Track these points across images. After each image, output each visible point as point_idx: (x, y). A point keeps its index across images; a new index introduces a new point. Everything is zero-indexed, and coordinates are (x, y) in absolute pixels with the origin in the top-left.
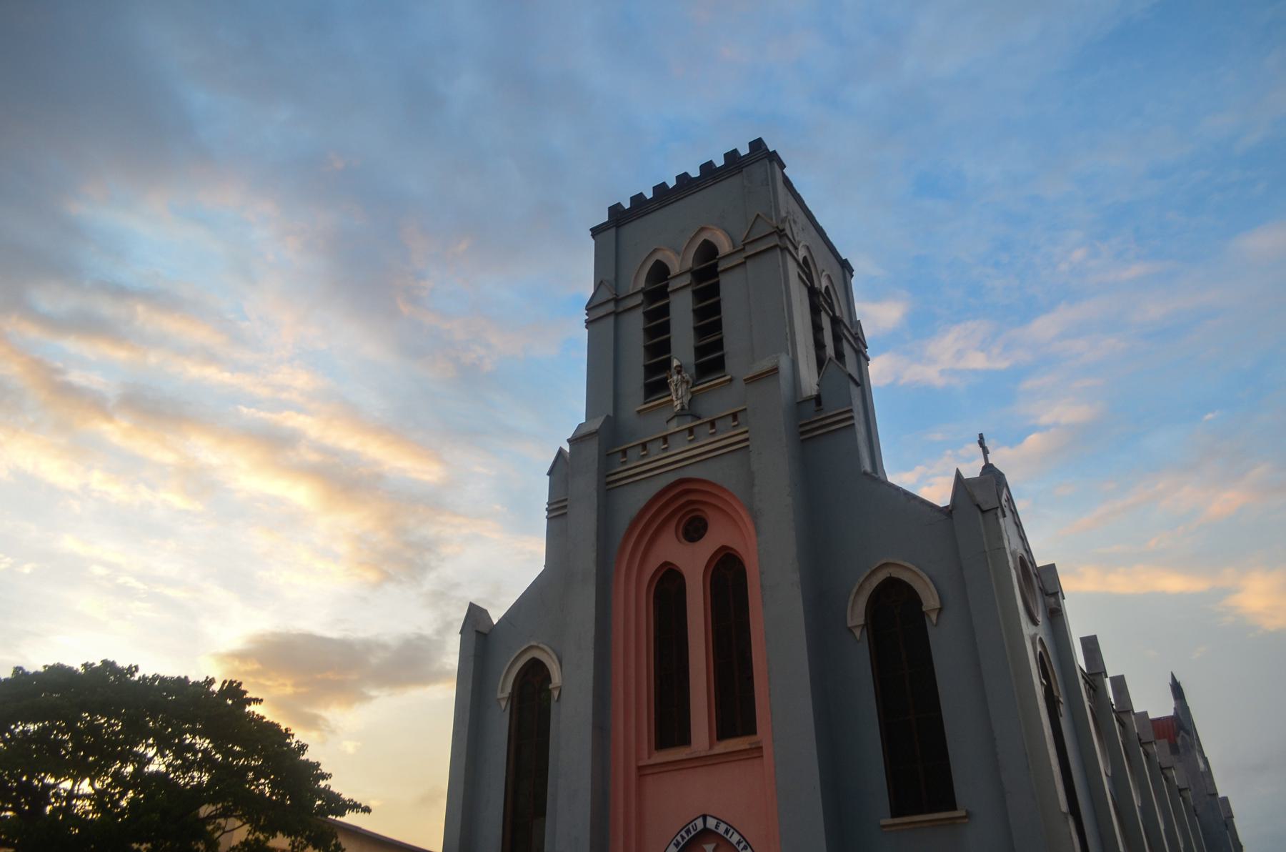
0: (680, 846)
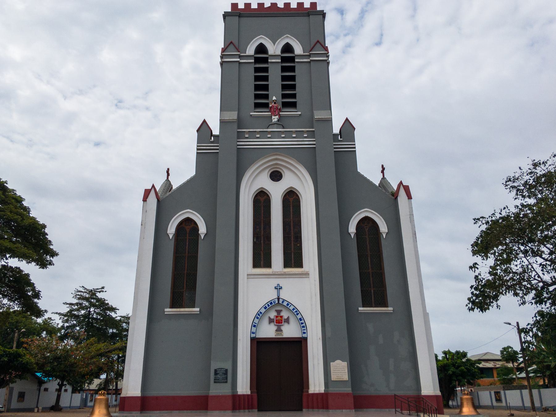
0: (267, 309)
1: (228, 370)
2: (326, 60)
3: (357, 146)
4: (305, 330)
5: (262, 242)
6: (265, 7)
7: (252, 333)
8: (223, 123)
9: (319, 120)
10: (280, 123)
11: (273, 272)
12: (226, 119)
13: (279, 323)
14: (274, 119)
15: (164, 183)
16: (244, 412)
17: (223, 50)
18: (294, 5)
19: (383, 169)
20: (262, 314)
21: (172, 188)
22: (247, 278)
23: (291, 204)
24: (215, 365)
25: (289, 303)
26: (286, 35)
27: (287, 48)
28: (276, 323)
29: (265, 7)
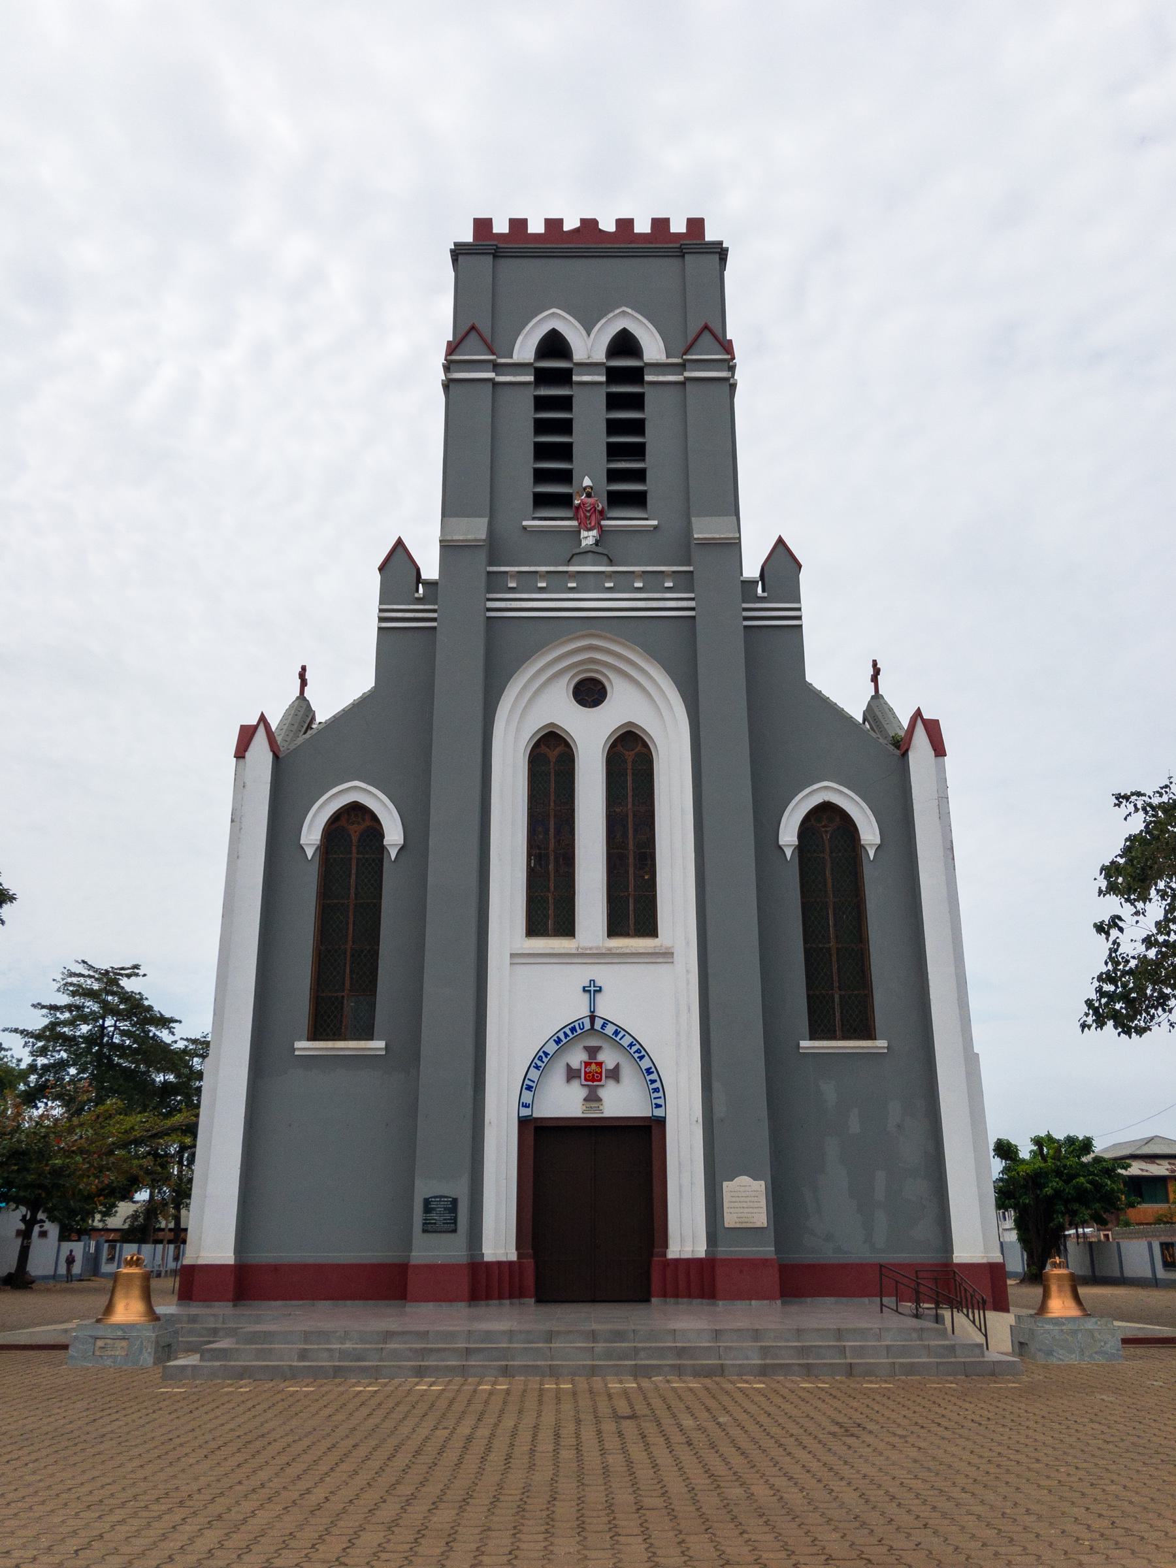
0: (562, 1043)
1: (459, 1201)
2: (726, 379)
3: (805, 613)
4: (660, 1098)
5: (551, 867)
6: (568, 226)
7: (523, 1106)
8: (448, 548)
9: (707, 544)
10: (600, 551)
11: (578, 949)
12: (456, 537)
14: (586, 537)
15: (291, 706)
16: (501, 1304)
17: (452, 348)
18: (642, 227)
19: (877, 672)
20: (549, 1057)
21: (313, 718)
23: (630, 767)
24: (424, 1189)
25: (619, 1029)
26: (621, 307)
27: (624, 344)
28: (586, 1080)
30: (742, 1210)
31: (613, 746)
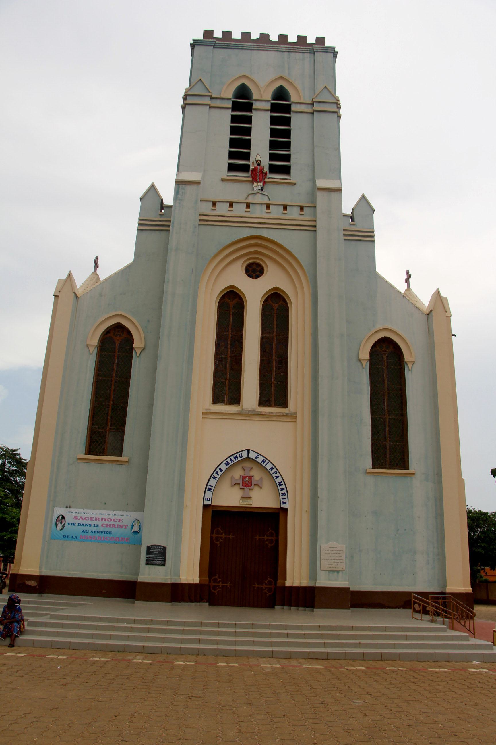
0: (230, 465)
4: (286, 499)
5: (228, 366)
6: (253, 37)
7: (206, 500)
13: (247, 486)
14: (256, 186)
17: (187, 90)
19: (409, 276)
22: (202, 418)
28: (243, 486)
29: (252, 39)
30: (331, 561)
31: (266, 300)
